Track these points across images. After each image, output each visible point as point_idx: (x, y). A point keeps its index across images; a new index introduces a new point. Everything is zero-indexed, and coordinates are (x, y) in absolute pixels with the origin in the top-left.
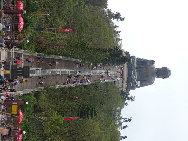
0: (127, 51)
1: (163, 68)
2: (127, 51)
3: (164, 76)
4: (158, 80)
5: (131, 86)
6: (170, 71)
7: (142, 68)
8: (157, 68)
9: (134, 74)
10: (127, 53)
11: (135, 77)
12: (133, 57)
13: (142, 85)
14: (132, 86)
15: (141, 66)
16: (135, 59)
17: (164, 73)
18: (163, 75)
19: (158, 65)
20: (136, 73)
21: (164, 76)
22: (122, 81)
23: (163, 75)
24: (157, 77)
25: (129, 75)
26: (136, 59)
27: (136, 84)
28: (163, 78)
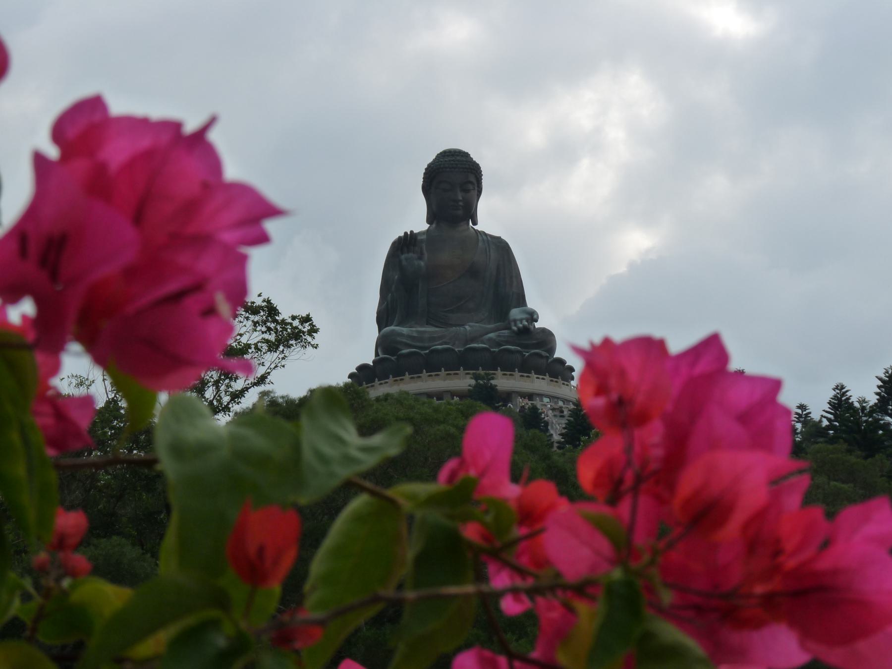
3: (471, 187)
4: (491, 216)
11: (492, 335)
12: (384, 344)
16: (401, 335)
19: (415, 218)
20: (467, 327)
21: (471, 187)
24: (475, 223)
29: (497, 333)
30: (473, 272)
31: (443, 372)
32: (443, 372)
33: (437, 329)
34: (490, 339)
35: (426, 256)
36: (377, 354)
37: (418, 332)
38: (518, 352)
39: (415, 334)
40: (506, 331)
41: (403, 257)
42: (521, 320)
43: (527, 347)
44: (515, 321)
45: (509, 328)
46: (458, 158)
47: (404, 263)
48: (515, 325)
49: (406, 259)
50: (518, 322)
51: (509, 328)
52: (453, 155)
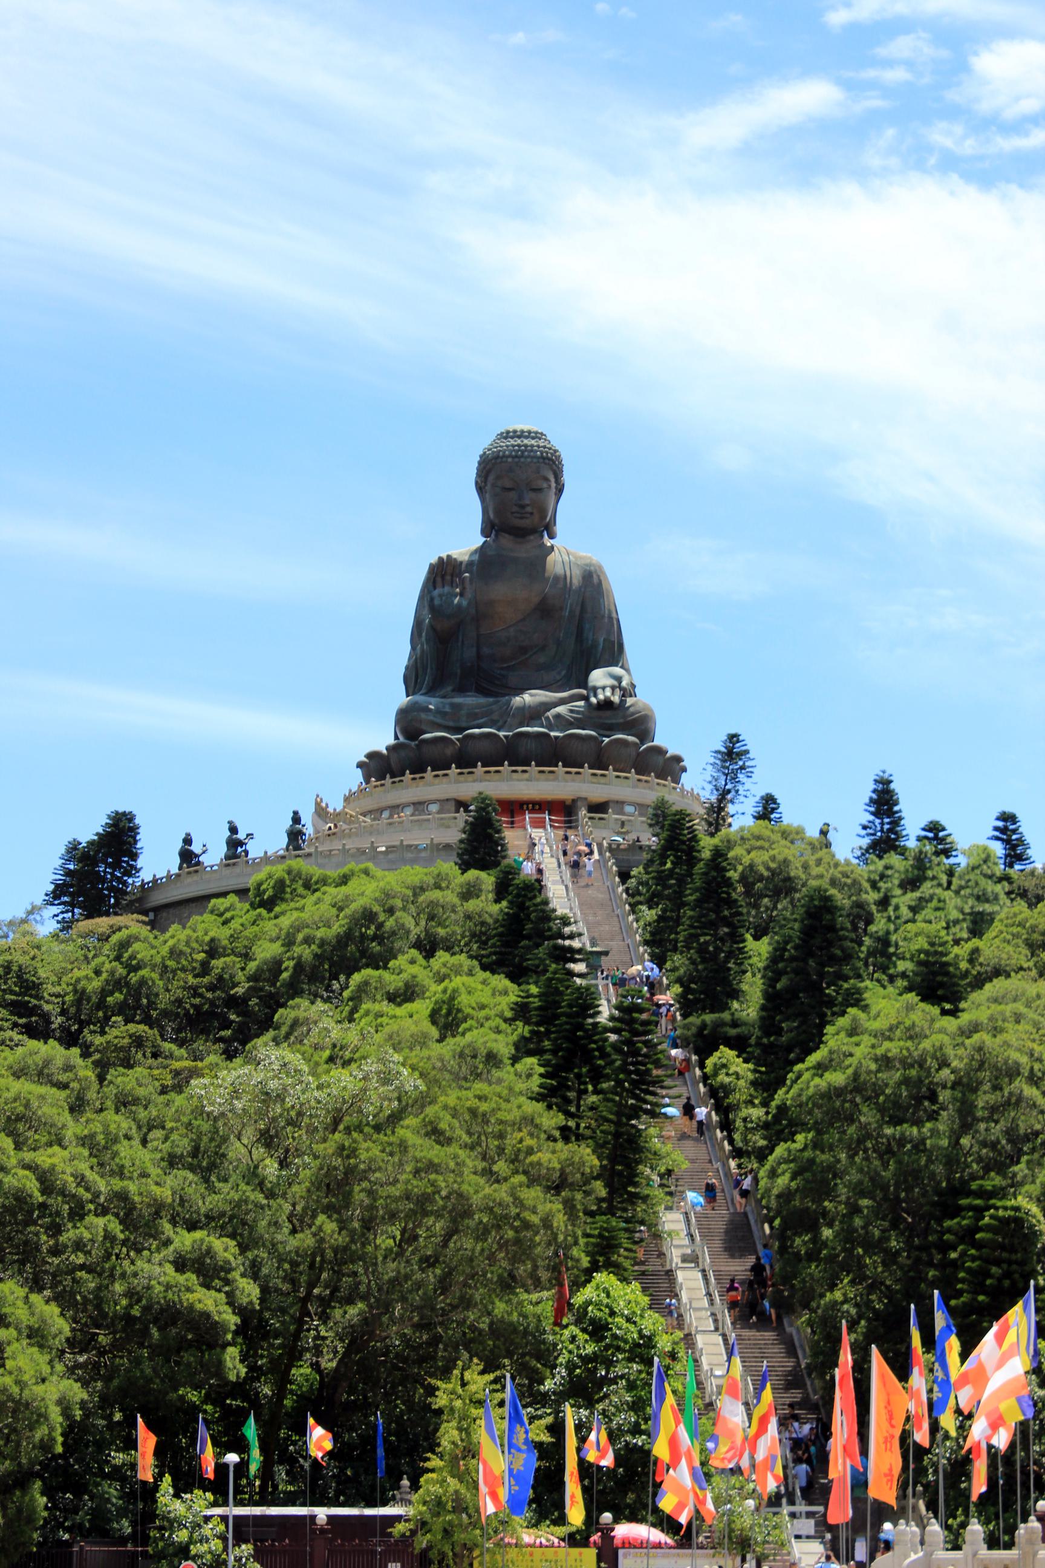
0: (360, 765)
1: (480, 489)
2: (360, 765)
5: (631, 738)
6: (506, 435)
7: (486, 651)
8: (485, 532)
9: (535, 714)
10: (378, 767)
11: (561, 709)
12: (408, 722)
13: (614, 653)
14: (620, 738)
15: (470, 653)
17: (518, 485)
18: (539, 490)
22: (598, 808)
23: (539, 490)
24: (552, 536)
25: (552, 754)
26: (419, 698)
27: (616, 699)
28: (560, 491)
29: (568, 706)
30: (545, 610)
31: (480, 769)
32: (480, 769)
33: (482, 700)
34: (558, 716)
35: (469, 594)
36: (396, 738)
37: (452, 705)
38: (590, 737)
39: (447, 709)
40: (582, 703)
41: (436, 593)
42: (604, 688)
43: (611, 729)
44: (595, 690)
45: (586, 698)
46: (526, 441)
47: (437, 602)
48: (595, 696)
49: (440, 596)
50: (600, 691)
51: (586, 698)
52: (519, 437)
